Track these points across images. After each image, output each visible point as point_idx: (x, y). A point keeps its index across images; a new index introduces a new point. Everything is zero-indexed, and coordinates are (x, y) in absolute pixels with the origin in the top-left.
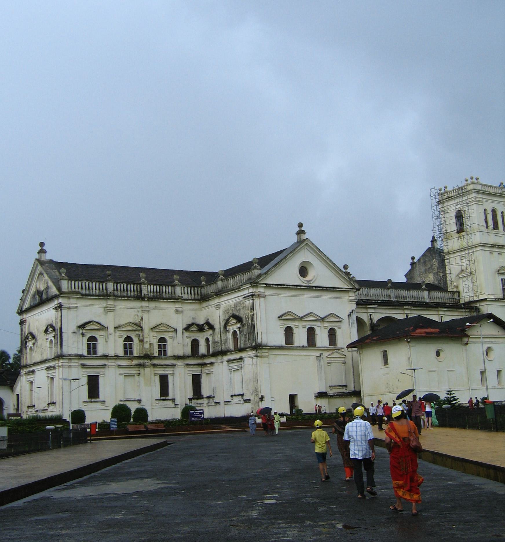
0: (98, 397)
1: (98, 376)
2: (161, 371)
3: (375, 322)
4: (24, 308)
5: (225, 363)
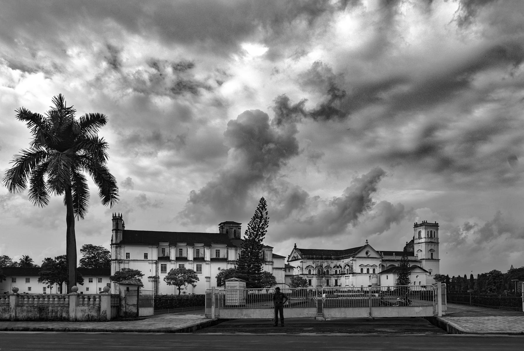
0: (311, 285)
1: (311, 280)
2: (327, 278)
3: (388, 266)
4: (289, 261)
5: (344, 277)
